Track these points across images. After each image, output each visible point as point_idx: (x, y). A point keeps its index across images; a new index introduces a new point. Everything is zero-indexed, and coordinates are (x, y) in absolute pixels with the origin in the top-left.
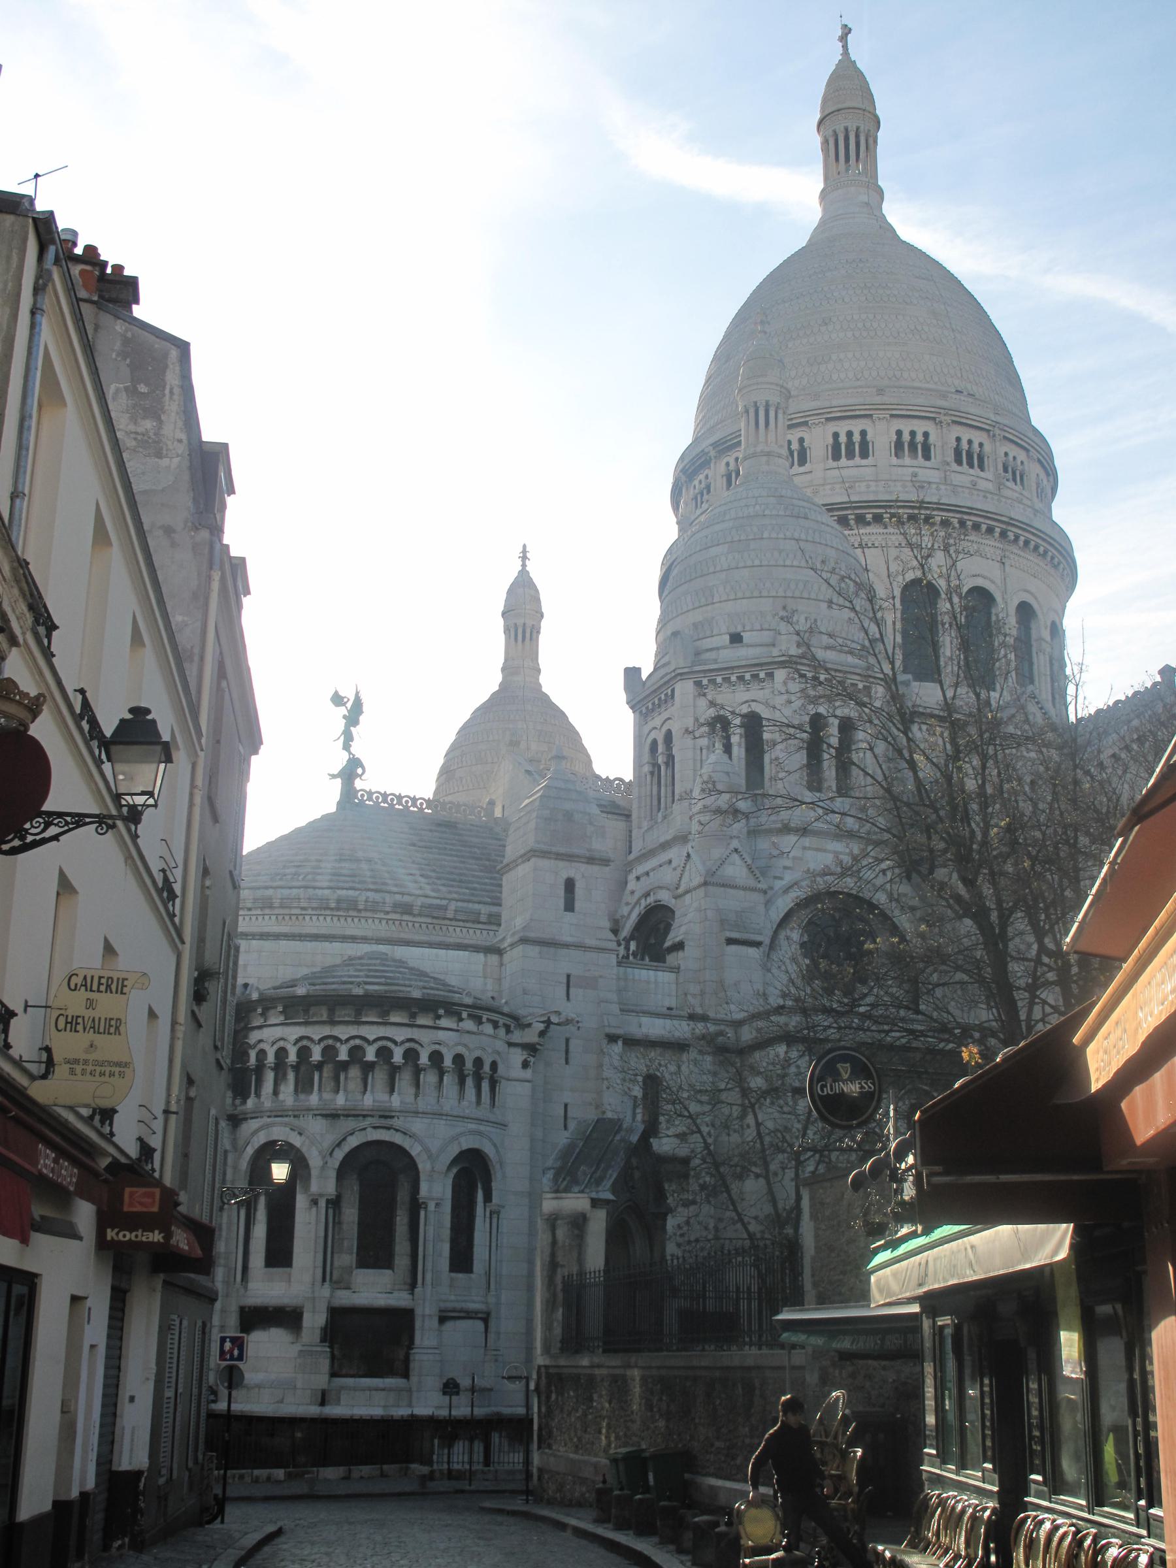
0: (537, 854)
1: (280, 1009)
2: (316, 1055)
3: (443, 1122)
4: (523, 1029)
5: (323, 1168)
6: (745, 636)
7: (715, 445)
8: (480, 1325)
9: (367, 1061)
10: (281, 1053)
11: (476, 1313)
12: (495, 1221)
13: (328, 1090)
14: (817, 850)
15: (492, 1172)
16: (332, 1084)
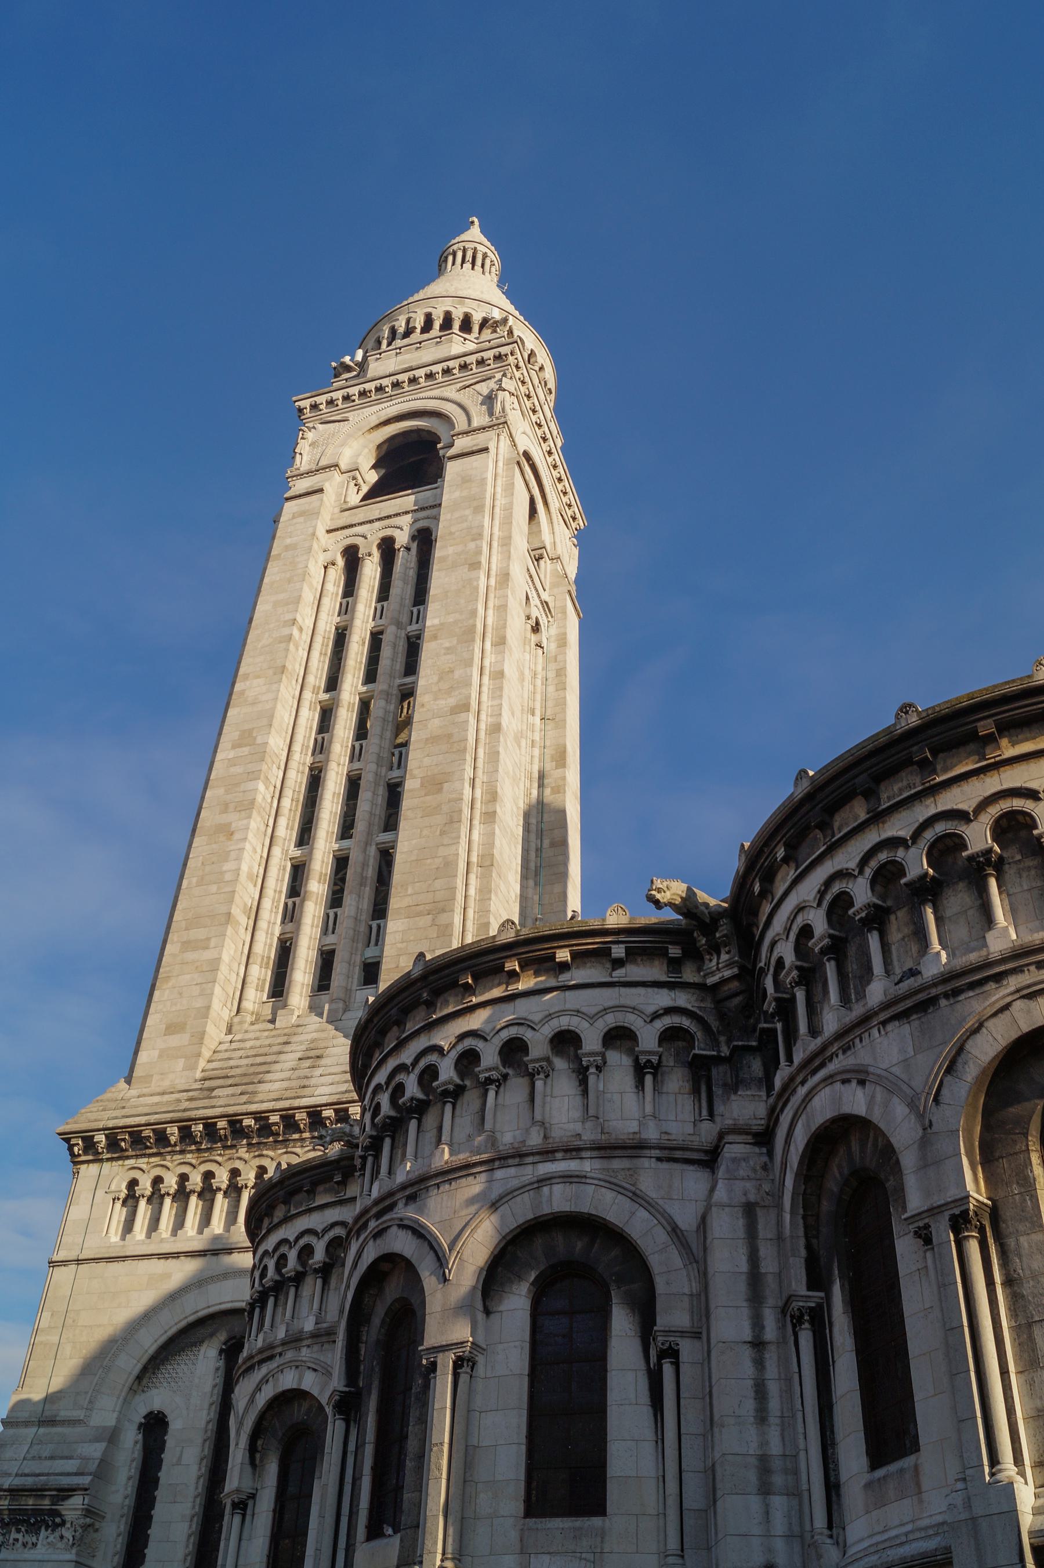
1: (781, 853)
9: (971, 858)
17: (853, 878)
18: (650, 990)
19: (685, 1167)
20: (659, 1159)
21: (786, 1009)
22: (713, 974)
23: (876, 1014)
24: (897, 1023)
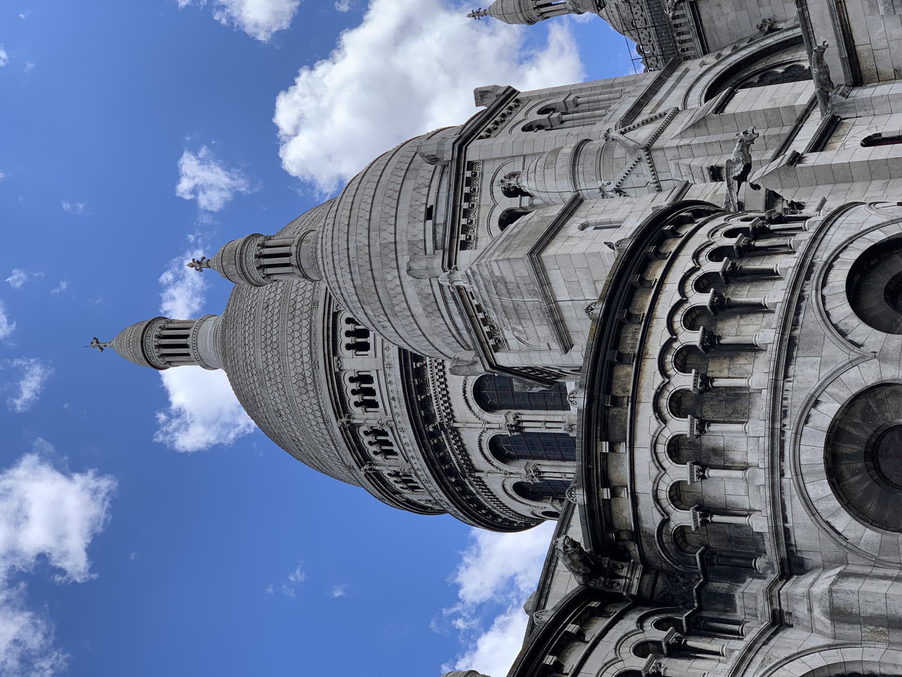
1: (605, 447)
2: (684, 381)
5: (880, 356)
6: (431, 202)
7: (338, 416)
9: (712, 302)
10: (676, 449)
13: (749, 368)
16: (742, 361)
17: (668, 386)
18: (615, 627)
19: (778, 636)
20: (764, 644)
21: (705, 509)
22: (630, 586)
23: (776, 380)
24: (791, 367)
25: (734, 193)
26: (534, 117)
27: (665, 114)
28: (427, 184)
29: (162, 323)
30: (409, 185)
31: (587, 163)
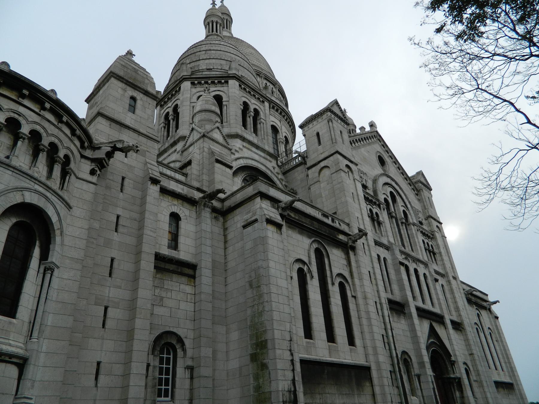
0: (115, 76)
3: (10, 173)
4: (94, 151)
8: (13, 371)
11: (11, 356)
12: (48, 276)
14: (248, 149)
15: (52, 236)
25: (106, 145)
26: (252, 107)
27: (228, 145)
28: (223, 68)
29: (229, 19)
30: (223, 62)
31: (204, 115)
